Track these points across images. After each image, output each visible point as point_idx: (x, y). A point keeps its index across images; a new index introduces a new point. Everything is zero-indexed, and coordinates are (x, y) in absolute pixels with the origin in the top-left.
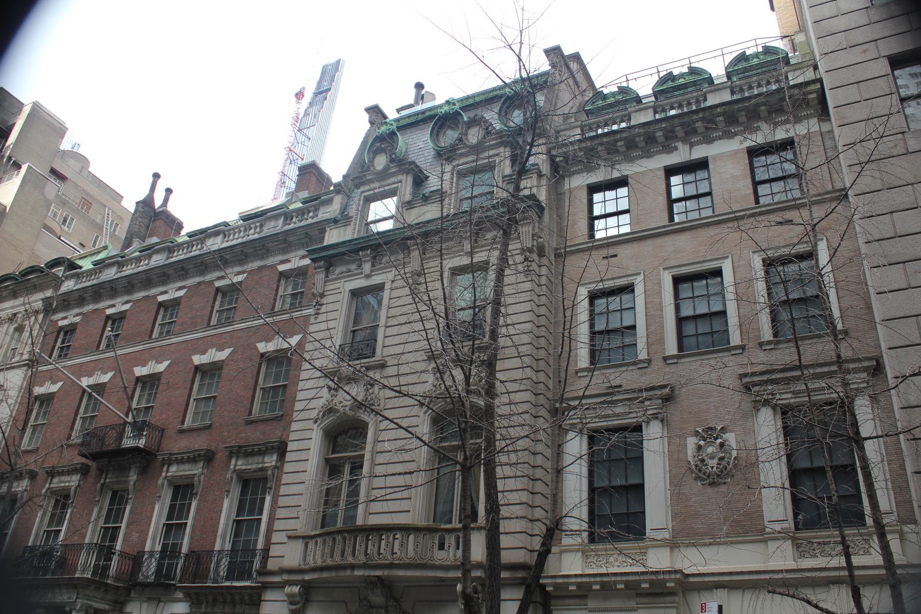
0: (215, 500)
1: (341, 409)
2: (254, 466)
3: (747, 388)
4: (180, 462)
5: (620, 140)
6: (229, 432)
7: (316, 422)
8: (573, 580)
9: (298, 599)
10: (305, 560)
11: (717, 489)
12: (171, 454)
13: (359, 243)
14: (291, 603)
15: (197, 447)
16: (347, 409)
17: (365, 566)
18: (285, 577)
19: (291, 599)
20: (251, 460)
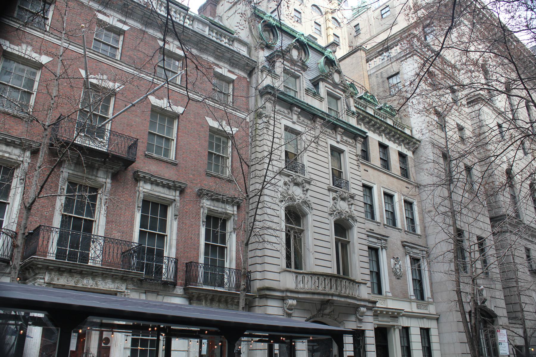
0: (192, 225)
1: (297, 201)
2: (220, 210)
3: (404, 246)
4: (157, 184)
5: (368, 118)
6: (194, 175)
7: (282, 201)
8: (380, 309)
9: (293, 307)
10: (297, 286)
11: (399, 280)
12: (152, 176)
13: (297, 102)
14: (288, 309)
15: (167, 176)
16: (300, 201)
17: (339, 296)
18: (289, 294)
19: (290, 307)
20: (216, 204)
